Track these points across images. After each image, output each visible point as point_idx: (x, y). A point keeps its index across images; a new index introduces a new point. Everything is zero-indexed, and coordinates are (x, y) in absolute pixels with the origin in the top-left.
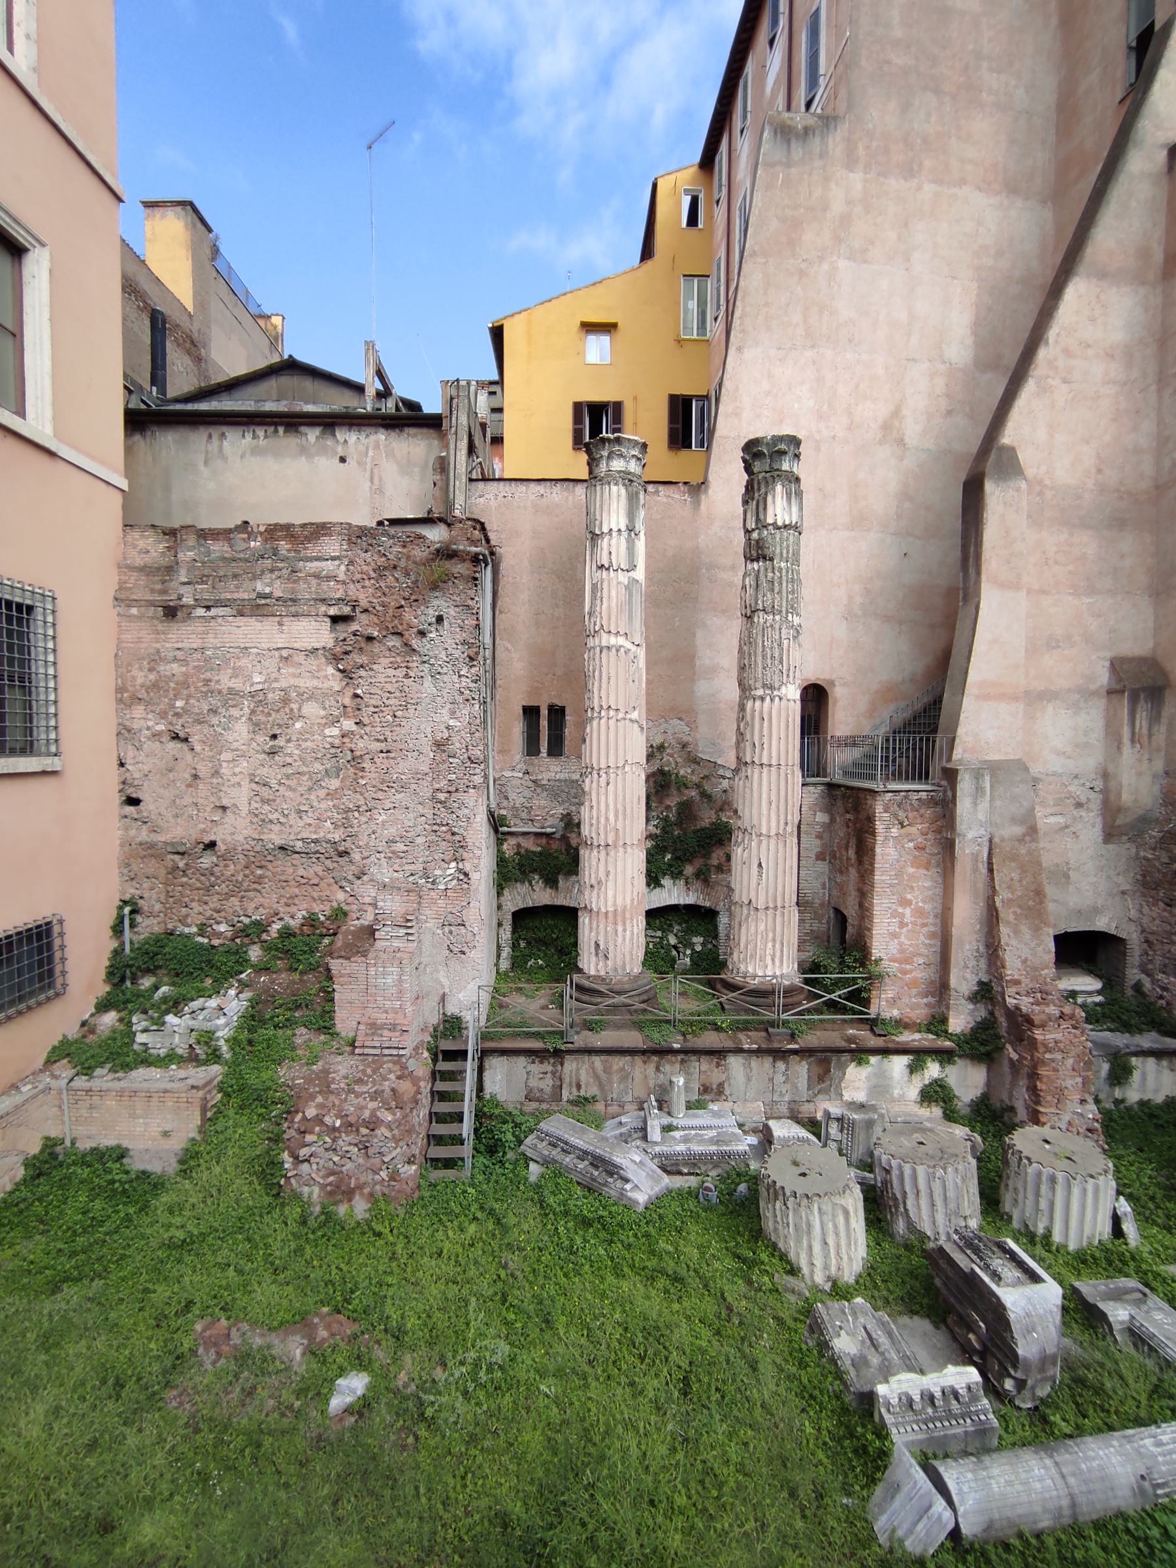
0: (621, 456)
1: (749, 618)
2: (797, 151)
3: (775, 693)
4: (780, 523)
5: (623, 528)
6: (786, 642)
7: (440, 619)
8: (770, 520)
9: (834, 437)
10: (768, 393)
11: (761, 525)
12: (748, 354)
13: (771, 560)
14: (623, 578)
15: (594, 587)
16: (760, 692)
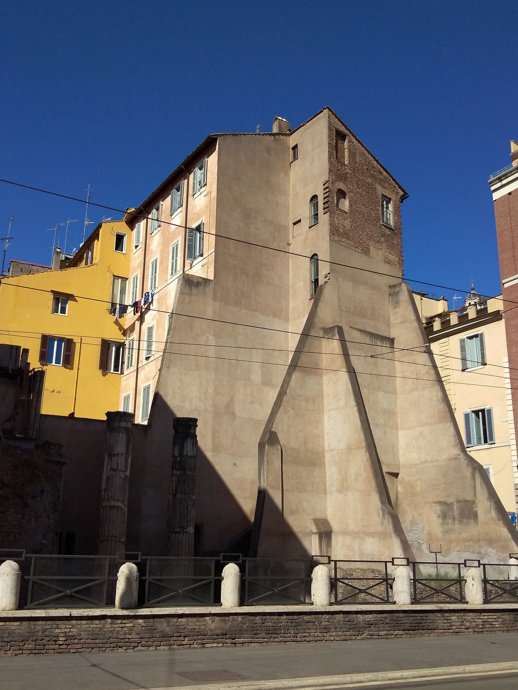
0: (125, 421)
1: (174, 495)
2: (194, 291)
3: (185, 530)
4: (189, 455)
5: (124, 452)
6: (190, 507)
7: (42, 491)
8: (185, 453)
9: (206, 410)
10: (179, 388)
11: (181, 454)
12: (172, 370)
13: (185, 470)
14: (122, 475)
15: (108, 478)
16: (177, 530)
